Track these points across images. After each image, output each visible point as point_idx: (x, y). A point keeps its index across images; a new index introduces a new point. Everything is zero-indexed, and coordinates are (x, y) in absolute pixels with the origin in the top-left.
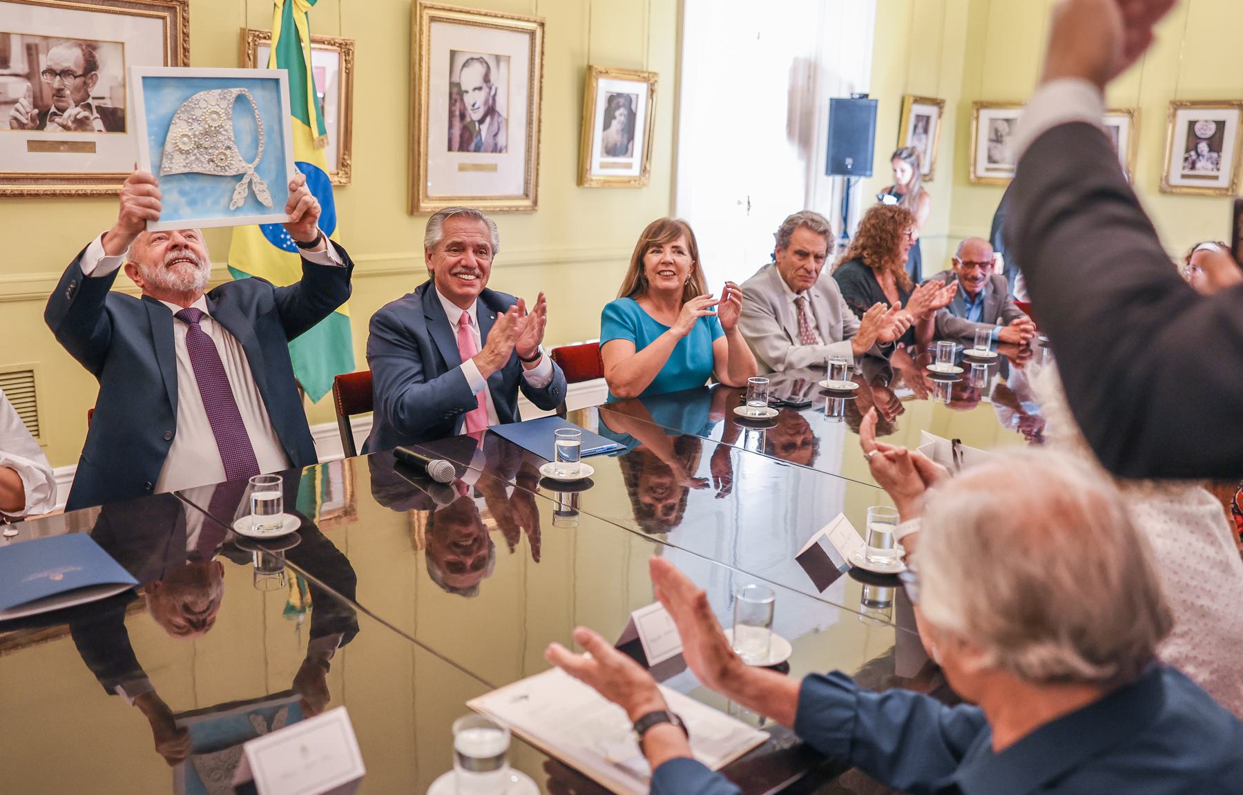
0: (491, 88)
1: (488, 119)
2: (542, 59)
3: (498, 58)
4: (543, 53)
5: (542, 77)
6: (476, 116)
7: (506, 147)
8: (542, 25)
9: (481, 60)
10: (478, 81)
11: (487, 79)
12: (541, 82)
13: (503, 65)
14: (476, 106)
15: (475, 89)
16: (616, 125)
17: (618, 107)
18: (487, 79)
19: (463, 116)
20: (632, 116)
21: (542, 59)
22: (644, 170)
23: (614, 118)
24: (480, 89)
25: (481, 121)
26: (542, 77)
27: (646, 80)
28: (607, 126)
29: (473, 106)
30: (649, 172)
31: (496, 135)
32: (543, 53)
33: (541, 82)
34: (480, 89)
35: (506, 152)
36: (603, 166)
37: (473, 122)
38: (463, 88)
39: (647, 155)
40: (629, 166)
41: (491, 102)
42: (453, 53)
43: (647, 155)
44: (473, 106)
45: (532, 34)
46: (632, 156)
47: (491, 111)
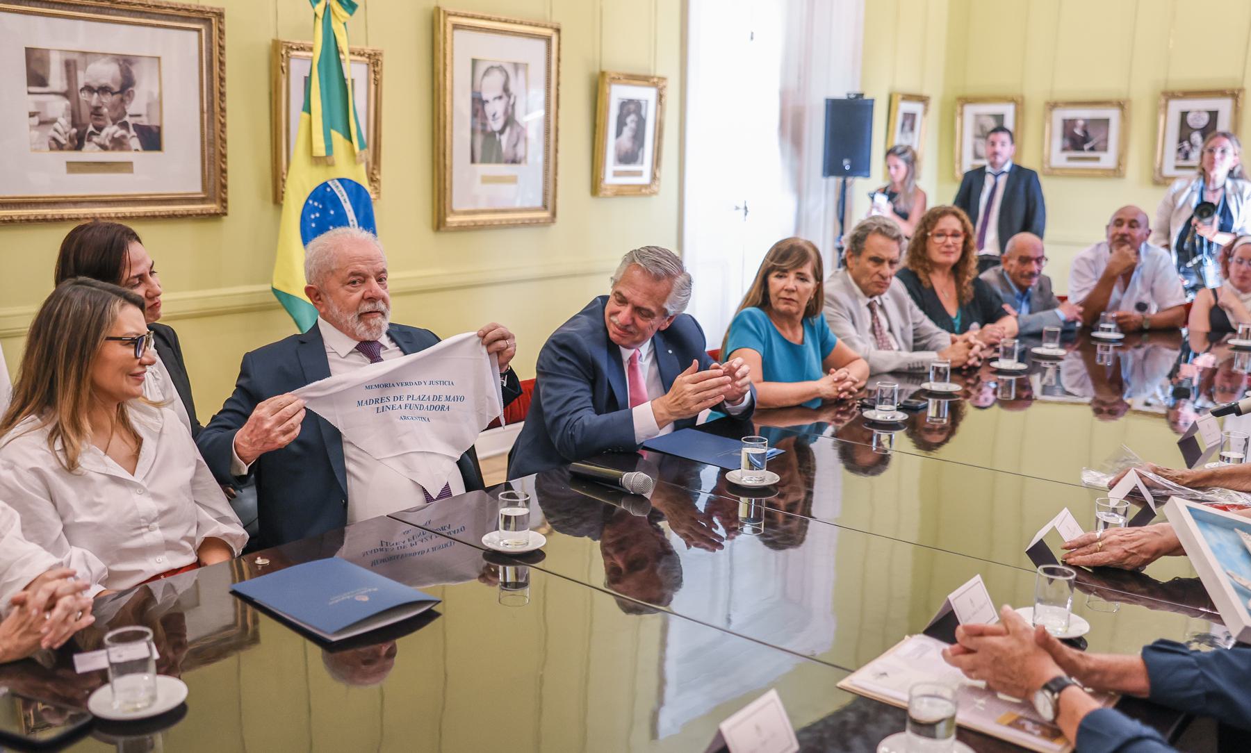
0: (509, 96)
1: (508, 130)
2: (558, 66)
3: (516, 66)
4: (559, 60)
5: (558, 84)
6: (496, 125)
7: (525, 157)
8: (558, 31)
9: (501, 68)
10: (499, 92)
11: (506, 89)
12: (558, 90)
13: (521, 74)
14: (496, 116)
15: (495, 98)
16: (627, 132)
17: (629, 114)
18: (506, 89)
19: (484, 125)
20: (641, 123)
21: (558, 66)
22: (654, 177)
23: (625, 124)
24: (500, 98)
25: (502, 132)
26: (558, 84)
27: (655, 85)
28: (619, 133)
29: (494, 115)
30: (659, 179)
31: (515, 146)
32: (559, 60)
33: (558, 90)
34: (500, 98)
35: (526, 162)
36: (617, 174)
37: (493, 134)
38: (485, 97)
39: (657, 161)
40: (639, 174)
41: (510, 110)
42: (474, 62)
43: (657, 161)
44: (494, 115)
45: (548, 40)
46: (642, 163)
47: (510, 121)
